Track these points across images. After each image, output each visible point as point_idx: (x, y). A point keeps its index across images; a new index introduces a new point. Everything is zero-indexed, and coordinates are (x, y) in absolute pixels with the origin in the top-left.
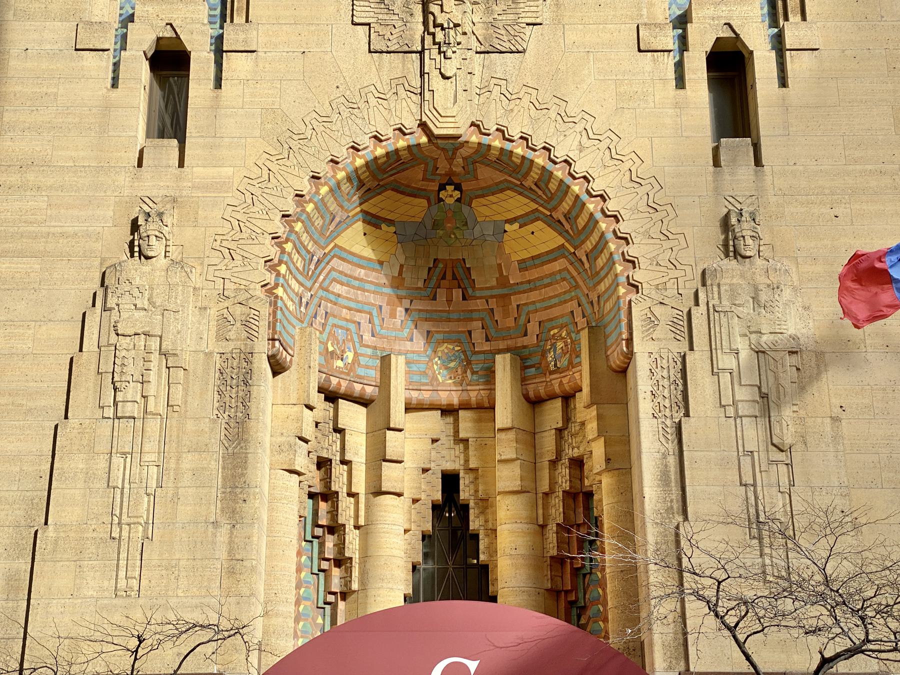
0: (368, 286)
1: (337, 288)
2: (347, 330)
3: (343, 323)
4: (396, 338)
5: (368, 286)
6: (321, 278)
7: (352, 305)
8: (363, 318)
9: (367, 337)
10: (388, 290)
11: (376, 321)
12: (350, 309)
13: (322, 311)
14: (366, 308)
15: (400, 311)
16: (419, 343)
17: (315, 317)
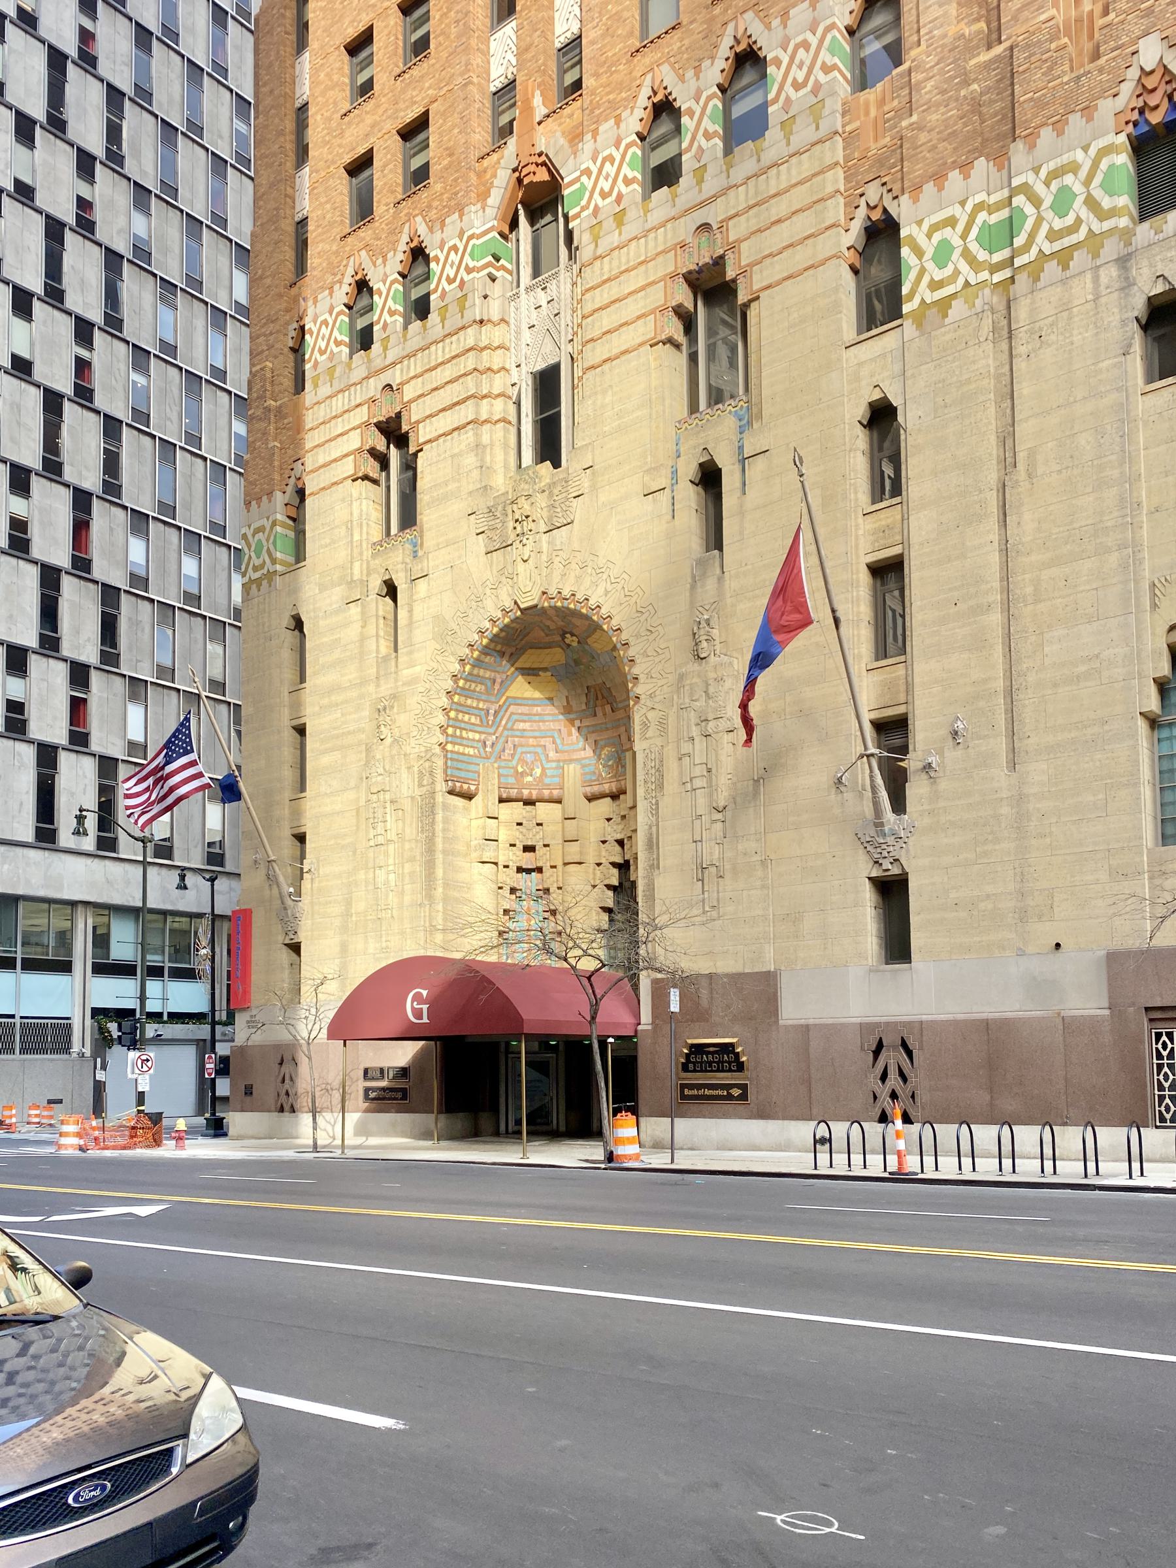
0: (546, 718)
1: (521, 726)
2: (535, 753)
3: (532, 749)
4: (574, 751)
5: (546, 718)
6: (504, 722)
7: (537, 734)
8: (547, 741)
9: (552, 754)
10: (561, 717)
11: (558, 741)
12: (535, 737)
13: (510, 744)
14: (549, 734)
15: (574, 731)
16: (589, 752)
17: (504, 750)
